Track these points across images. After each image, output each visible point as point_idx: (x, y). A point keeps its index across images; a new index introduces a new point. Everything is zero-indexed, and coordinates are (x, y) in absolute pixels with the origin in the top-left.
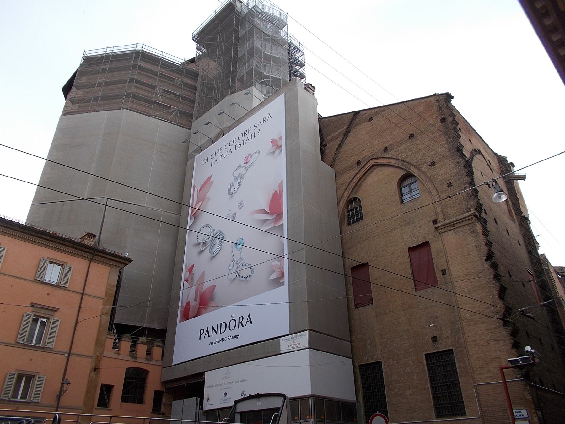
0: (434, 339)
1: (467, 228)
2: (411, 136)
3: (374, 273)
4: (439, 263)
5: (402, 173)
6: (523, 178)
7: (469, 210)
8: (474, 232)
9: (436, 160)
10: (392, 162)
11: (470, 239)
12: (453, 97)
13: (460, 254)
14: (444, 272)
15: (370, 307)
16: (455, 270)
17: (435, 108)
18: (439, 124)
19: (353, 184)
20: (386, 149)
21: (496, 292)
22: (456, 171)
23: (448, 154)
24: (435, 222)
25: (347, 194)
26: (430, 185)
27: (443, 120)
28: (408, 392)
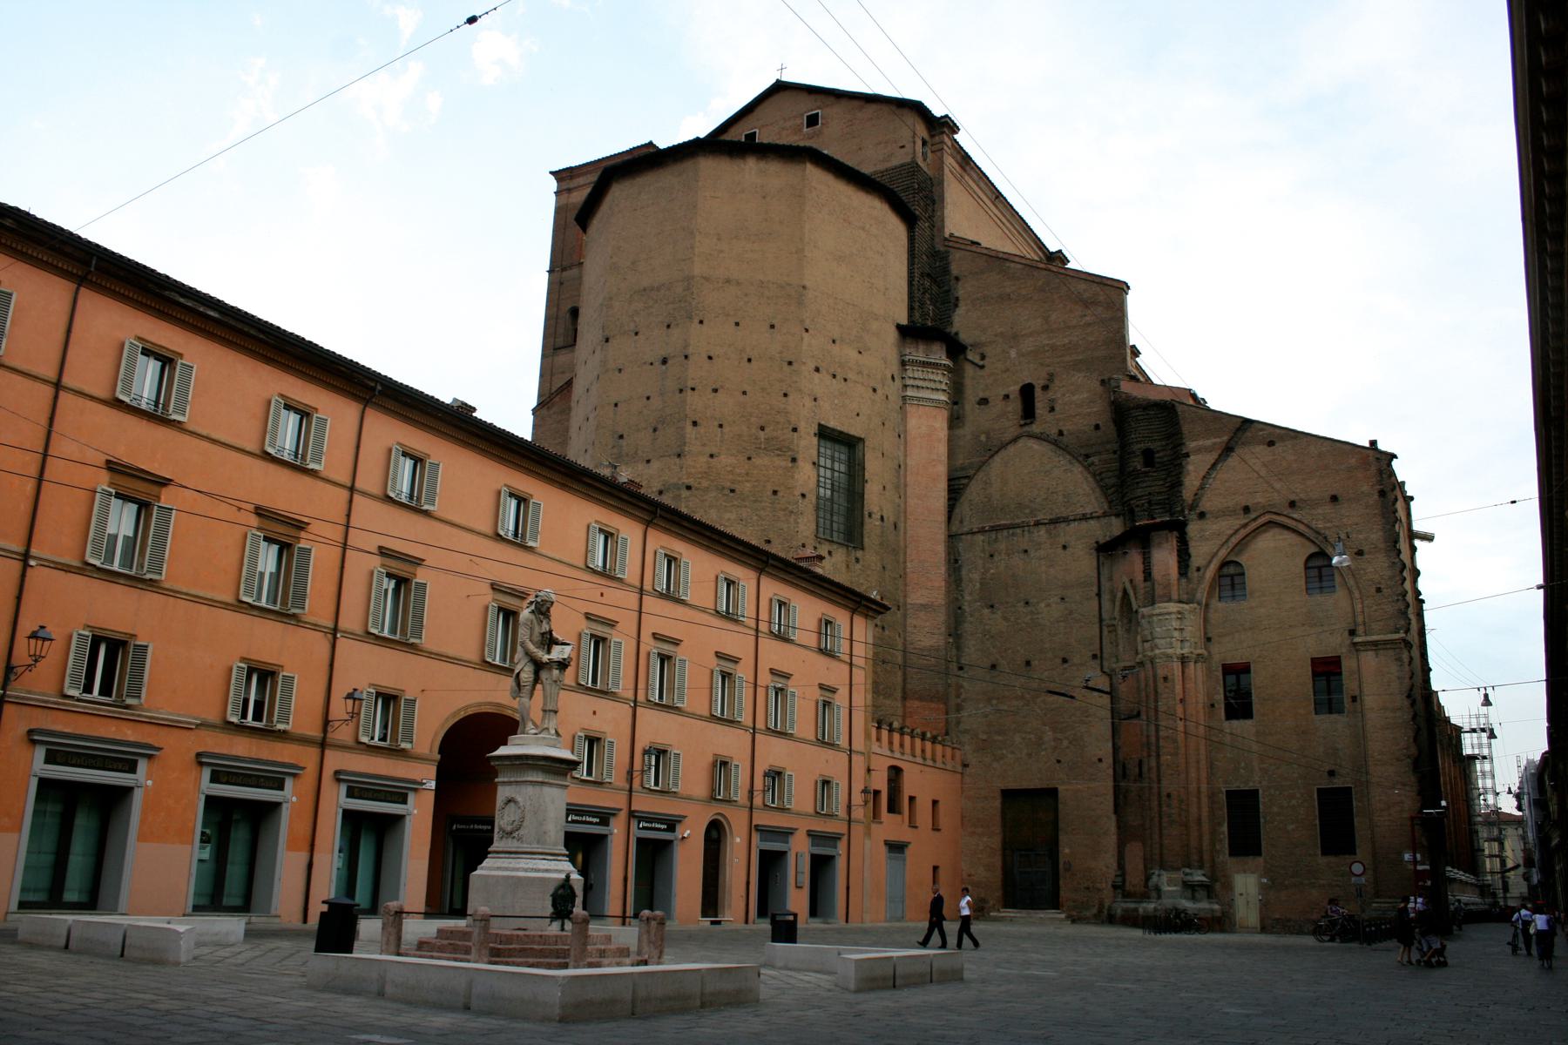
0: (1331, 773)
1: (1391, 652)
2: (1334, 499)
3: (1259, 680)
4: (1349, 684)
5: (1314, 549)
6: (1429, 538)
7: (1397, 631)
8: (1399, 659)
9: (1366, 549)
10: (1301, 528)
11: (1394, 668)
12: (1394, 456)
13: (1372, 678)
14: (1354, 699)
15: (1249, 722)
16: (1370, 701)
17: (1373, 469)
18: (1376, 496)
19: (1234, 540)
20: (1292, 504)
21: (1411, 734)
22: (1389, 573)
23: (1382, 546)
24: (1352, 633)
25: (1223, 553)
26: (1351, 582)
27: (1382, 493)
28: (1290, 827)
